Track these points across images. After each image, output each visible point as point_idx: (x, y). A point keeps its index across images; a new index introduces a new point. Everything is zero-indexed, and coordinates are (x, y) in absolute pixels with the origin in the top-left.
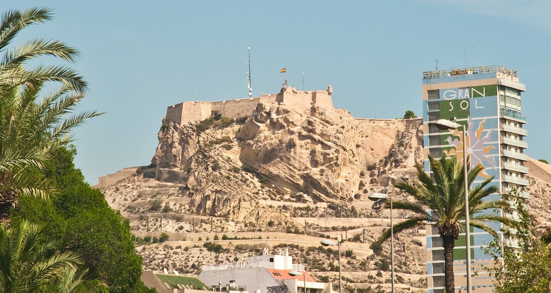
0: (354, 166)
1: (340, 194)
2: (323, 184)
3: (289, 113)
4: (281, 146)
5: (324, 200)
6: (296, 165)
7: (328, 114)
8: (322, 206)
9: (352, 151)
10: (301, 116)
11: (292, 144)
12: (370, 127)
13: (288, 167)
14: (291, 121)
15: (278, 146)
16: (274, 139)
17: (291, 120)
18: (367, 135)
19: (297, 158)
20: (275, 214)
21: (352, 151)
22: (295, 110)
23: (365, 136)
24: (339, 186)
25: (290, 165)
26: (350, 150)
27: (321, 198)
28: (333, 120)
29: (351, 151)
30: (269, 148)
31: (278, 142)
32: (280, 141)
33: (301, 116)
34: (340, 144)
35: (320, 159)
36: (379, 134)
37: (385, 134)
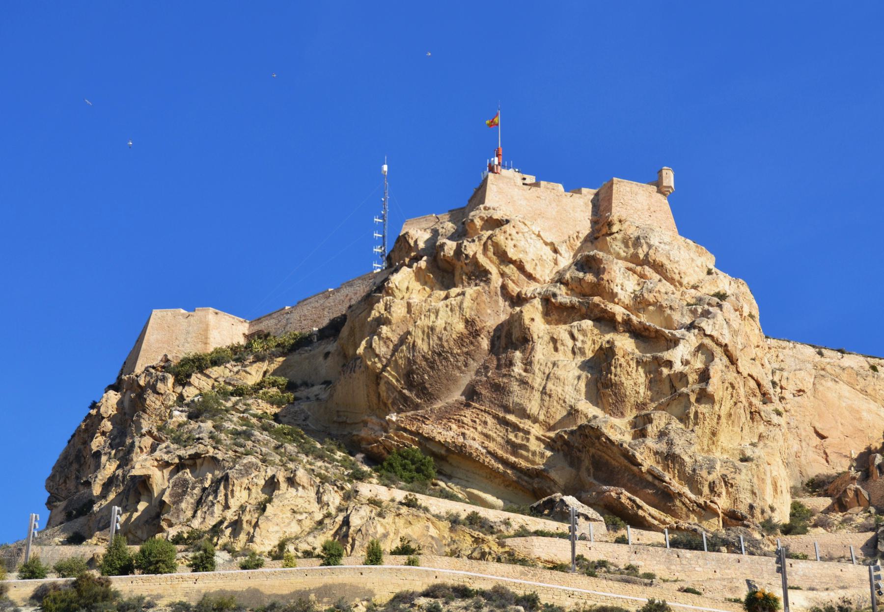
0: (771, 428)
1: (723, 503)
2: (647, 462)
3: (506, 227)
4: (472, 343)
5: (650, 519)
6: (533, 406)
9: (759, 385)
10: (556, 251)
11: (516, 334)
13: (495, 417)
14: (514, 258)
15: (461, 340)
16: (441, 314)
17: (512, 254)
18: (801, 387)
19: (537, 381)
20: (428, 527)
21: (759, 385)
23: (791, 388)
26: (749, 375)
27: (640, 512)
29: (752, 384)
30: (423, 346)
31: (460, 327)
32: (469, 323)
33: (556, 251)
34: (715, 334)
36: (845, 389)
37: (864, 392)
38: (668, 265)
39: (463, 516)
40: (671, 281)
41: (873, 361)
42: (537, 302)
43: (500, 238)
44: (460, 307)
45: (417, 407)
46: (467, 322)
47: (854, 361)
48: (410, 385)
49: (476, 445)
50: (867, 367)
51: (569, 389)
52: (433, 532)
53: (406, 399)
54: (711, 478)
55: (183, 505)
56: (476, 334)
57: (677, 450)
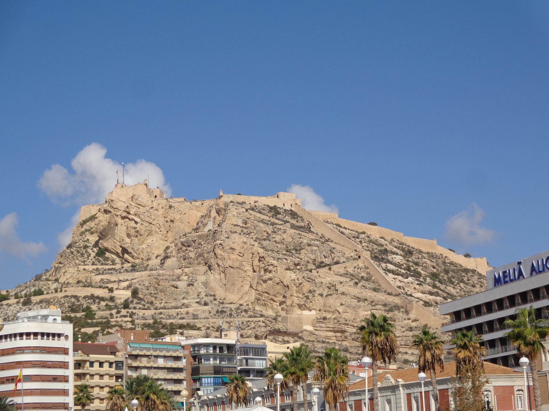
5: (130, 261)
6: (118, 239)
7: (140, 199)
8: (127, 266)
12: (188, 207)
15: (108, 226)
19: (118, 233)
22: (120, 200)
23: (183, 213)
24: (140, 250)
25: (115, 239)
28: (145, 204)
29: (158, 225)
35: (132, 232)
36: (194, 211)
37: (199, 211)
38: (141, 204)
39: (96, 268)
40: (143, 207)
41: (202, 202)
42: (119, 216)
43: (112, 205)
44: (106, 220)
45: (104, 239)
46: (108, 222)
47: (198, 203)
48: (102, 236)
49: (110, 247)
50: (201, 204)
51: (123, 234)
52: (87, 275)
53: (102, 238)
54: (138, 252)
55: (57, 273)
56: (110, 224)
57: (134, 247)
